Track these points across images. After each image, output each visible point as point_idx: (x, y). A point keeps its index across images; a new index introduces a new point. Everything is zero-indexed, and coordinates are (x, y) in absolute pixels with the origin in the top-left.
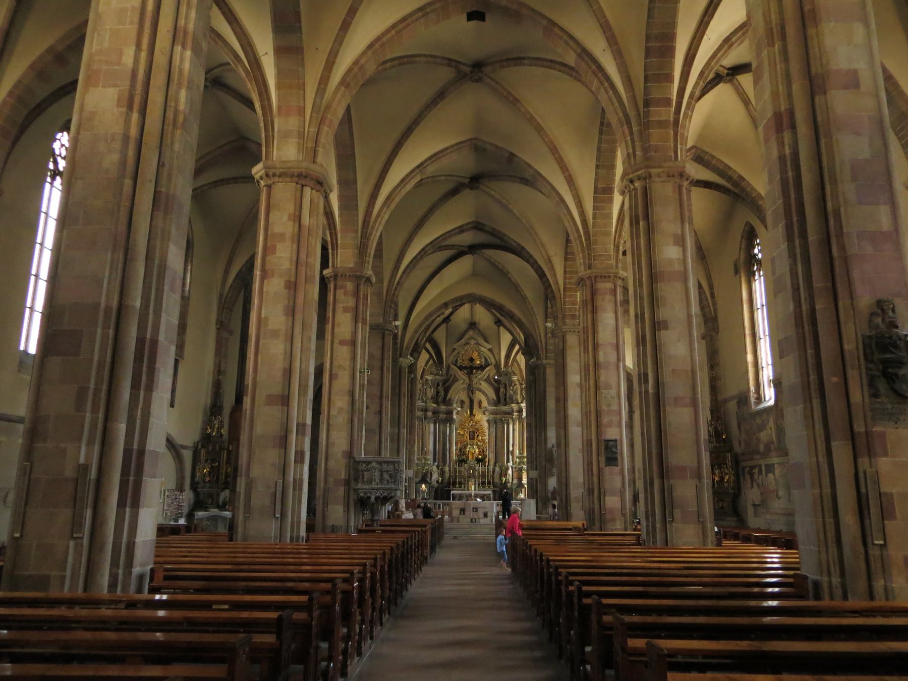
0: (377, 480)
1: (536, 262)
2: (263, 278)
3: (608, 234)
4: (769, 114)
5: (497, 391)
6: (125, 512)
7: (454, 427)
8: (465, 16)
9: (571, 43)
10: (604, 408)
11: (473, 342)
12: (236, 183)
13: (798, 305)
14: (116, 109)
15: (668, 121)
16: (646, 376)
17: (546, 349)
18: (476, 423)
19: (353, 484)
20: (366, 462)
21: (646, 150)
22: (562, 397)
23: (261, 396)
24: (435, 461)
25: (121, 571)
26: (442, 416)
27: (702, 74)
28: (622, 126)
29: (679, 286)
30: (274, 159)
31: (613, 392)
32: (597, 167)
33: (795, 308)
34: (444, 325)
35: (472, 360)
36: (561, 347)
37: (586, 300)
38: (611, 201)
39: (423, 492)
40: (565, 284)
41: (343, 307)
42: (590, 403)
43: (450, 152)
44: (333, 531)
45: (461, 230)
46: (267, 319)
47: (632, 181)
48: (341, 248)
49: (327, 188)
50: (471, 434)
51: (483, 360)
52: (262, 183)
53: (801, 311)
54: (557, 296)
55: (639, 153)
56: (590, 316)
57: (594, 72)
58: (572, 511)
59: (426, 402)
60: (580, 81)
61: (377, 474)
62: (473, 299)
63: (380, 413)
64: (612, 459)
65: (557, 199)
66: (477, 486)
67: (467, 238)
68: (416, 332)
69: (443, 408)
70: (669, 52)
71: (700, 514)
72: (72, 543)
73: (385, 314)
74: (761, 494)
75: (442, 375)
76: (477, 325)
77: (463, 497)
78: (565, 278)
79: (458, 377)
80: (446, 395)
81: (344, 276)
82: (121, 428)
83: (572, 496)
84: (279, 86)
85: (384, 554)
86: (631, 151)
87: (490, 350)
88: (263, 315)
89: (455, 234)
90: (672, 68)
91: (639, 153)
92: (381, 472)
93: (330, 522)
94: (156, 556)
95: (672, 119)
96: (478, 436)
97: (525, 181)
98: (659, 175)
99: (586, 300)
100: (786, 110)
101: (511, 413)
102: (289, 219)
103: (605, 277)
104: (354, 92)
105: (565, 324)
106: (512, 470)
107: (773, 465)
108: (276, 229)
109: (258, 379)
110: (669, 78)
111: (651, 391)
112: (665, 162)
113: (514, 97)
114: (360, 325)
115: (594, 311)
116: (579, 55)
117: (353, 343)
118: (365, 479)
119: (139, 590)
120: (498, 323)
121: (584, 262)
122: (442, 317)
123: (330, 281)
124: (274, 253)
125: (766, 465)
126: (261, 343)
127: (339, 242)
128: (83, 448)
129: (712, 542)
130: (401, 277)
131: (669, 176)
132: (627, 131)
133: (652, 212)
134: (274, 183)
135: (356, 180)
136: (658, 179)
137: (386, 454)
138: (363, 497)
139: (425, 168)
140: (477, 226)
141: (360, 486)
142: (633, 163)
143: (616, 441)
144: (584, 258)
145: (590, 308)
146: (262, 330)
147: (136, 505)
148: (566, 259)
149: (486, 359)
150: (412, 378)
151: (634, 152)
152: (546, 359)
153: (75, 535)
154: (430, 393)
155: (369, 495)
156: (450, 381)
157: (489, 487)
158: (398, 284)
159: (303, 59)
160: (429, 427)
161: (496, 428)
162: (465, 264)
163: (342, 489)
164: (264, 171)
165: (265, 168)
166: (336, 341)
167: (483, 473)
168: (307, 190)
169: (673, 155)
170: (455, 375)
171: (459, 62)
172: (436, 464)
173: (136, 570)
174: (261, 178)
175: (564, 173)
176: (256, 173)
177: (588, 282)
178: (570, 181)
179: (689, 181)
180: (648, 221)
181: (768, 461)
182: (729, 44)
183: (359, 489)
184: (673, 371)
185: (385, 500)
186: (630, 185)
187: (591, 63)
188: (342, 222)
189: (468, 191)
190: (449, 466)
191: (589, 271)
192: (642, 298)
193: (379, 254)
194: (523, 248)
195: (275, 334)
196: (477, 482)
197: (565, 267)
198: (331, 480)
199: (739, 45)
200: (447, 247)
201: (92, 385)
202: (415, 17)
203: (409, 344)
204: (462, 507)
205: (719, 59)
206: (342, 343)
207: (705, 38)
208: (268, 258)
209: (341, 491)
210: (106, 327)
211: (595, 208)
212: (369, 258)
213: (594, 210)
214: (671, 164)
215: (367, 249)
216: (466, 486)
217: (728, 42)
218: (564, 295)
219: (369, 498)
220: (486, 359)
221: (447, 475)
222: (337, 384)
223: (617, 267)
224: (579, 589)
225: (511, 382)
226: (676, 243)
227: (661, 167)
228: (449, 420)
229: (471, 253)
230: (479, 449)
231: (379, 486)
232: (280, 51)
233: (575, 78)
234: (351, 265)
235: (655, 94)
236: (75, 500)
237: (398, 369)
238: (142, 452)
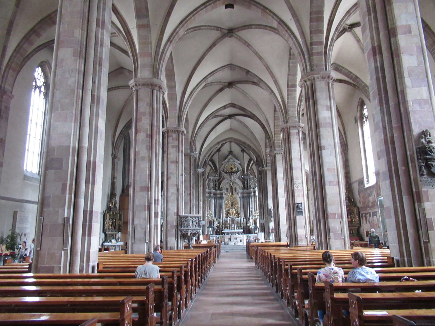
0: (191, 225)
1: (260, 121)
2: (136, 133)
3: (294, 107)
4: (370, 47)
5: (243, 183)
6: (85, 238)
7: (224, 200)
8: (224, 6)
9: (275, 17)
10: (295, 188)
12: (119, 89)
13: (385, 135)
14: (72, 58)
15: (321, 52)
16: (315, 172)
17: (266, 162)
18: (234, 199)
19: (179, 227)
20: (185, 217)
21: (311, 66)
22: (275, 184)
23: (137, 188)
24: (215, 217)
25: (85, 264)
26: (218, 196)
27: (337, 29)
28: (300, 55)
29: (330, 129)
30: (139, 77)
31: (300, 181)
32: (288, 75)
33: (384, 136)
34: (217, 153)
35: (232, 169)
36: (274, 161)
37: (285, 138)
38: (295, 91)
39: (210, 232)
40: (274, 131)
41: (172, 146)
42: (289, 186)
43: (219, 71)
44: (171, 249)
45: (225, 107)
46: (139, 152)
47: (305, 81)
48: (170, 118)
49: (163, 90)
52: (134, 89)
53: (387, 138)
54: (271, 137)
55: (308, 68)
56: (287, 145)
57: (286, 30)
58: (281, 237)
59: (210, 190)
60: (279, 35)
61: (190, 223)
62: (231, 140)
63: (190, 194)
64: (301, 213)
65: (270, 91)
67: (228, 111)
68: (205, 156)
69: (218, 192)
70: (320, 19)
71: (342, 234)
72: (63, 252)
73: (191, 148)
74: (371, 226)
75: (217, 177)
76: (233, 152)
78: (274, 128)
80: (219, 186)
81: (172, 131)
82: (82, 201)
83: (281, 230)
84: (139, 43)
85: (199, 256)
86: (305, 67)
87: (240, 164)
88: (137, 150)
89: (222, 110)
90: (322, 27)
91: (308, 68)
92: (192, 221)
93: (169, 245)
94: (98, 260)
95: (323, 51)
96: (235, 205)
97: (254, 83)
98: (318, 78)
99: (285, 138)
100: (377, 45)
101: (250, 193)
102: (147, 105)
103: (294, 127)
104: (174, 45)
105: (275, 150)
107: (376, 212)
108: (141, 110)
109: (136, 179)
110: (321, 32)
111: (318, 179)
112: (321, 71)
113: (248, 44)
114: (180, 154)
115: (289, 143)
116: (279, 23)
117: (178, 162)
118: (185, 225)
119: (93, 272)
120: (243, 151)
121: (284, 121)
122: (216, 149)
123: (165, 134)
124: (141, 121)
125: (373, 213)
126: (136, 163)
127: (169, 115)
128: (66, 210)
129: (348, 247)
130: (198, 131)
131: (322, 78)
132: (302, 58)
133: (316, 95)
134: (139, 89)
135: (176, 86)
136: (318, 80)
137: (193, 214)
138: (184, 233)
139: (207, 79)
140: (233, 105)
141: (183, 228)
142: (306, 73)
143: (301, 203)
144: (284, 118)
145: (287, 142)
146: (137, 157)
147: (90, 235)
148: (275, 119)
149: (238, 169)
150: (204, 178)
151: (306, 67)
152: (267, 167)
153: (64, 249)
154: (212, 185)
155: (187, 232)
157: (241, 228)
158: (196, 133)
159: (150, 30)
160: (212, 201)
161: (244, 201)
162: (226, 124)
163: (174, 230)
164: (134, 83)
165: (135, 81)
166: (169, 161)
168: (155, 92)
169: (324, 68)
170: (223, 177)
171: (222, 28)
172: (216, 218)
173: (91, 264)
174: (133, 86)
175: (273, 79)
176: (131, 84)
177: (286, 130)
178: (276, 82)
179: (332, 80)
180: (314, 99)
181: (374, 211)
182: (349, 14)
183: (182, 230)
184: (328, 169)
185: (194, 234)
186: (305, 83)
187: (284, 26)
188: (169, 106)
189: (227, 89)
190: (222, 219)
191: (286, 125)
192: (312, 136)
193: (187, 121)
194: (254, 115)
195: (143, 158)
197: (274, 123)
198: (169, 226)
199: (354, 14)
200: (218, 116)
201: (68, 182)
202: (202, 7)
203: (202, 162)
204: (230, 237)
205: (345, 21)
206: (172, 162)
207: (338, 11)
208: (138, 124)
209: (174, 231)
210: (73, 156)
211: (288, 95)
212: (183, 122)
213: (287, 95)
214: (324, 72)
215: (182, 118)
216: (230, 228)
217: (348, 13)
218: (274, 136)
219: (187, 234)
220: (238, 169)
221: (221, 223)
222: (170, 182)
223: (299, 122)
224: (291, 266)
225: (250, 179)
226: (327, 110)
227: (319, 74)
228: (221, 198)
229: (229, 118)
230: (236, 211)
231: (192, 228)
232: (139, 27)
233: (277, 34)
234: (175, 126)
235: (315, 39)
236: (64, 233)
237: (197, 175)
238: (91, 212)
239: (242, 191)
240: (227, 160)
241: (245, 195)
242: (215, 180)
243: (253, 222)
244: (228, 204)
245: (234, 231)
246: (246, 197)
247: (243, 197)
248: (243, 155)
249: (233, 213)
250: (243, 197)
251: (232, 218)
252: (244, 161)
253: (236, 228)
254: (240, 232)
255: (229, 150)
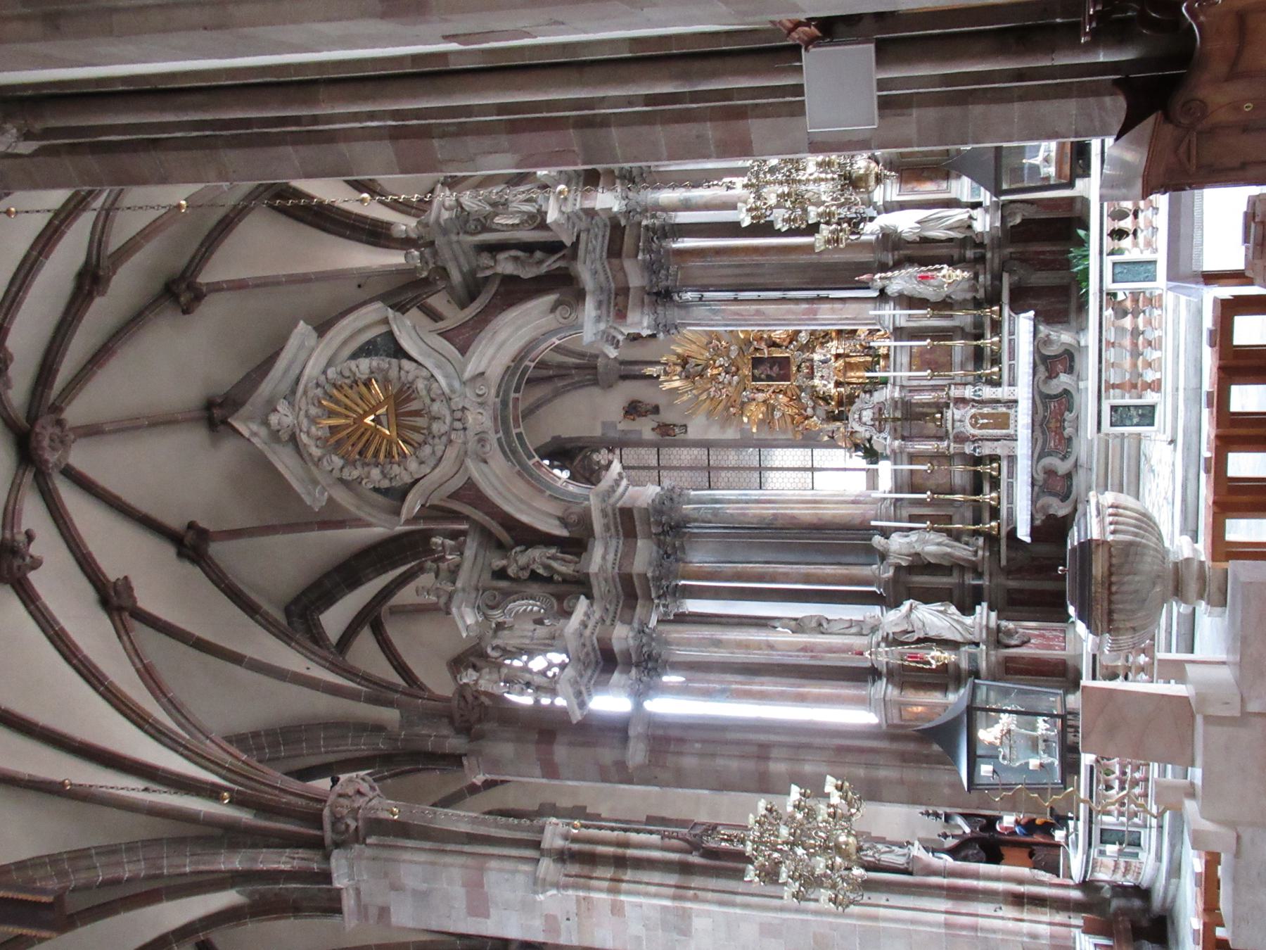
11: (283, 416)
26: (644, 557)
50: (761, 371)
51: (364, 365)
66: (988, 392)
69: (600, 559)
77: (1050, 472)
79: (457, 483)
106: (902, 206)
149: (367, 350)
156: (478, 515)
157: (996, 327)
167: (921, 361)
170: (454, 496)
190: (886, 533)
196: (968, 392)
220: (367, 350)
221: (932, 545)
239: (590, 307)
240: (284, 461)
241: (636, 279)
242: (487, 576)
243: (929, 190)
244: (771, 409)
245: (1023, 418)
246: (652, 268)
247: (662, 296)
248: (239, 286)
249: (849, 367)
250: (662, 296)
251: (879, 421)
252: (305, 279)
253: (998, 384)
254: (1039, 344)
255: (196, 437)
